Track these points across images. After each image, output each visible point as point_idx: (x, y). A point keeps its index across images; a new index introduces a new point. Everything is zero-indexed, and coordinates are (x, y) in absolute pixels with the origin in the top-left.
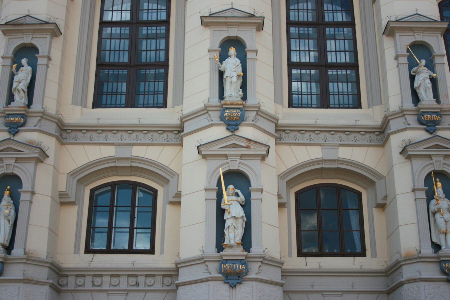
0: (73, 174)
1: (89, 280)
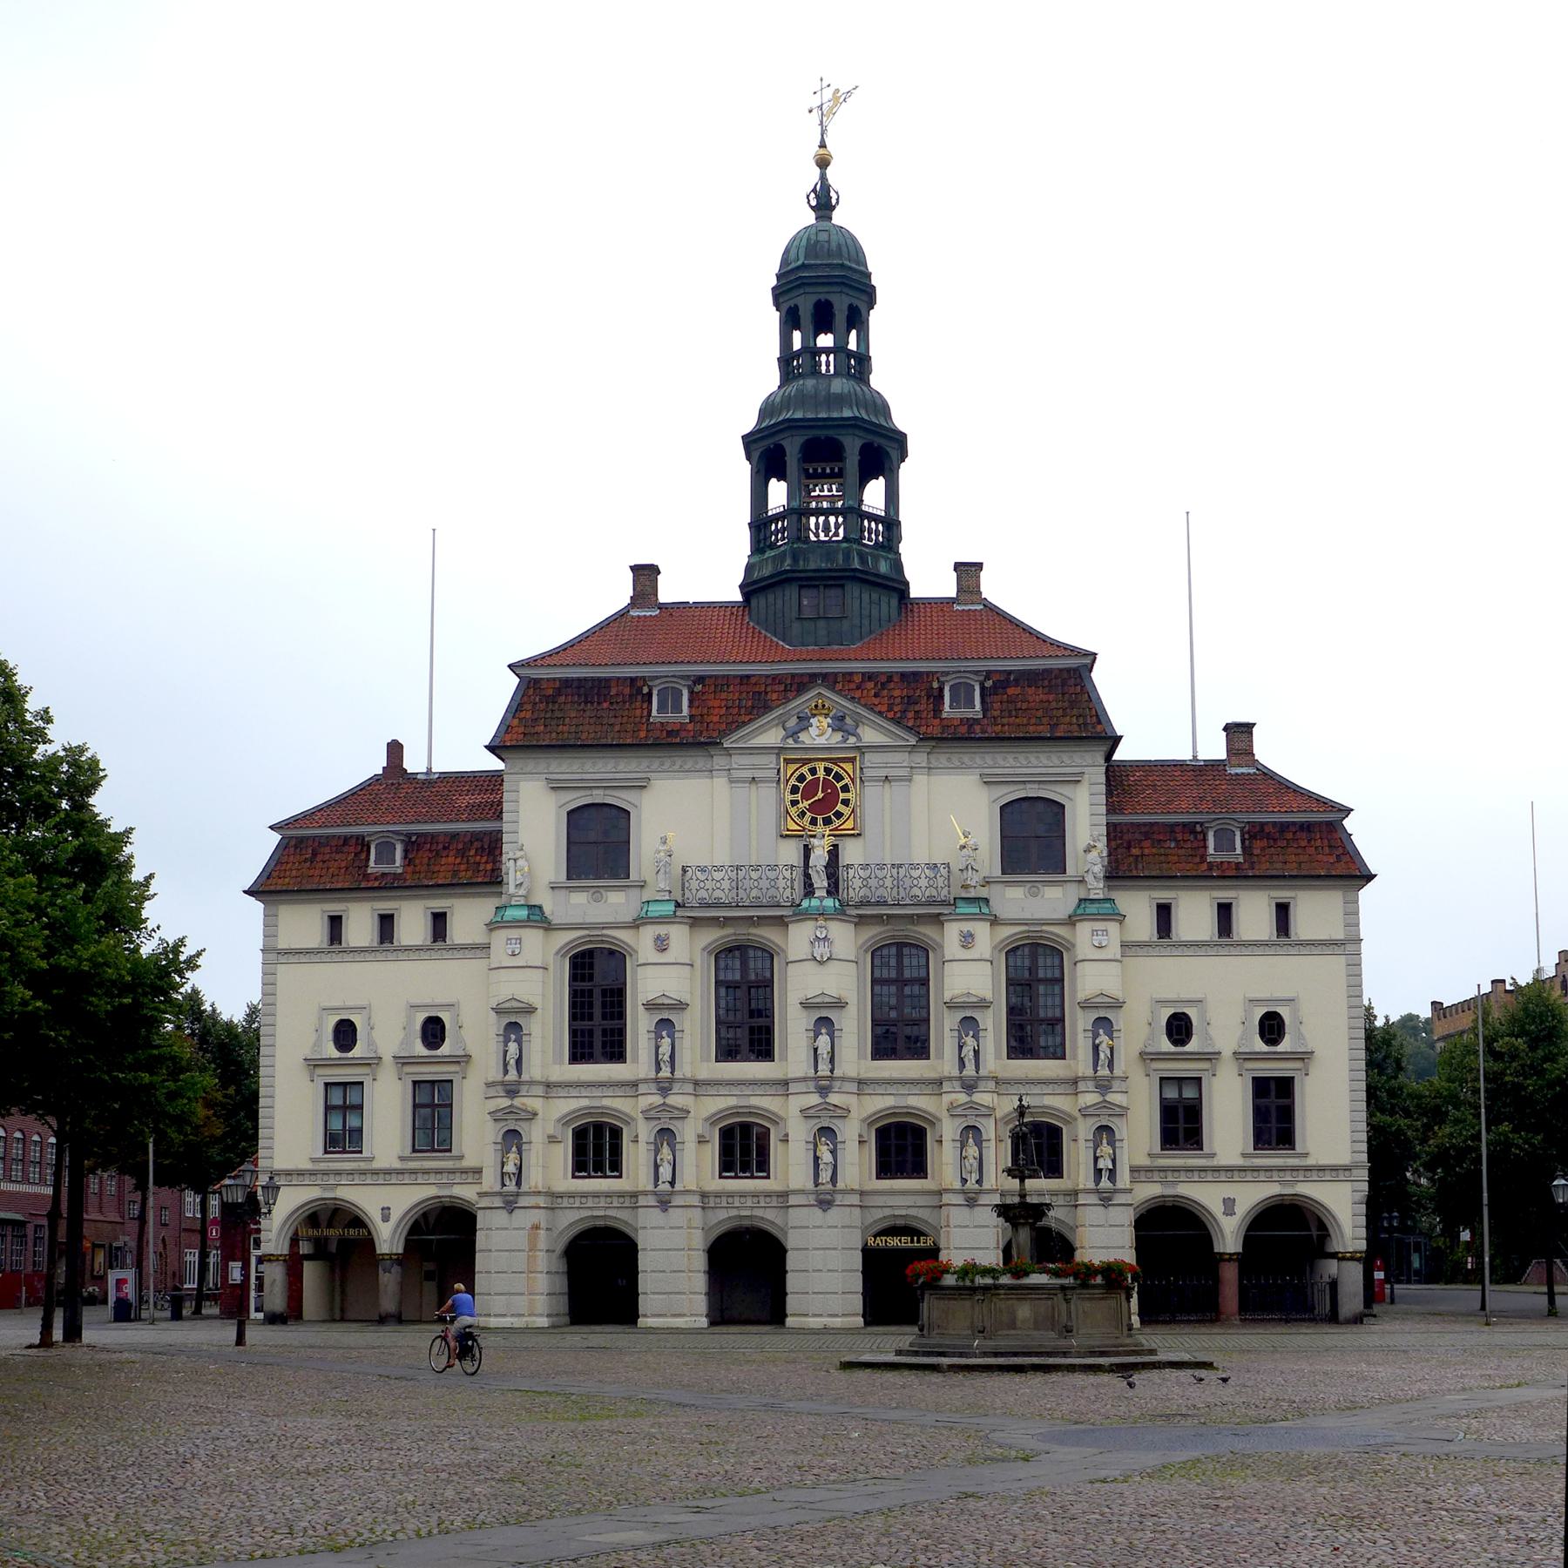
0: (706, 1120)
1: (724, 1199)
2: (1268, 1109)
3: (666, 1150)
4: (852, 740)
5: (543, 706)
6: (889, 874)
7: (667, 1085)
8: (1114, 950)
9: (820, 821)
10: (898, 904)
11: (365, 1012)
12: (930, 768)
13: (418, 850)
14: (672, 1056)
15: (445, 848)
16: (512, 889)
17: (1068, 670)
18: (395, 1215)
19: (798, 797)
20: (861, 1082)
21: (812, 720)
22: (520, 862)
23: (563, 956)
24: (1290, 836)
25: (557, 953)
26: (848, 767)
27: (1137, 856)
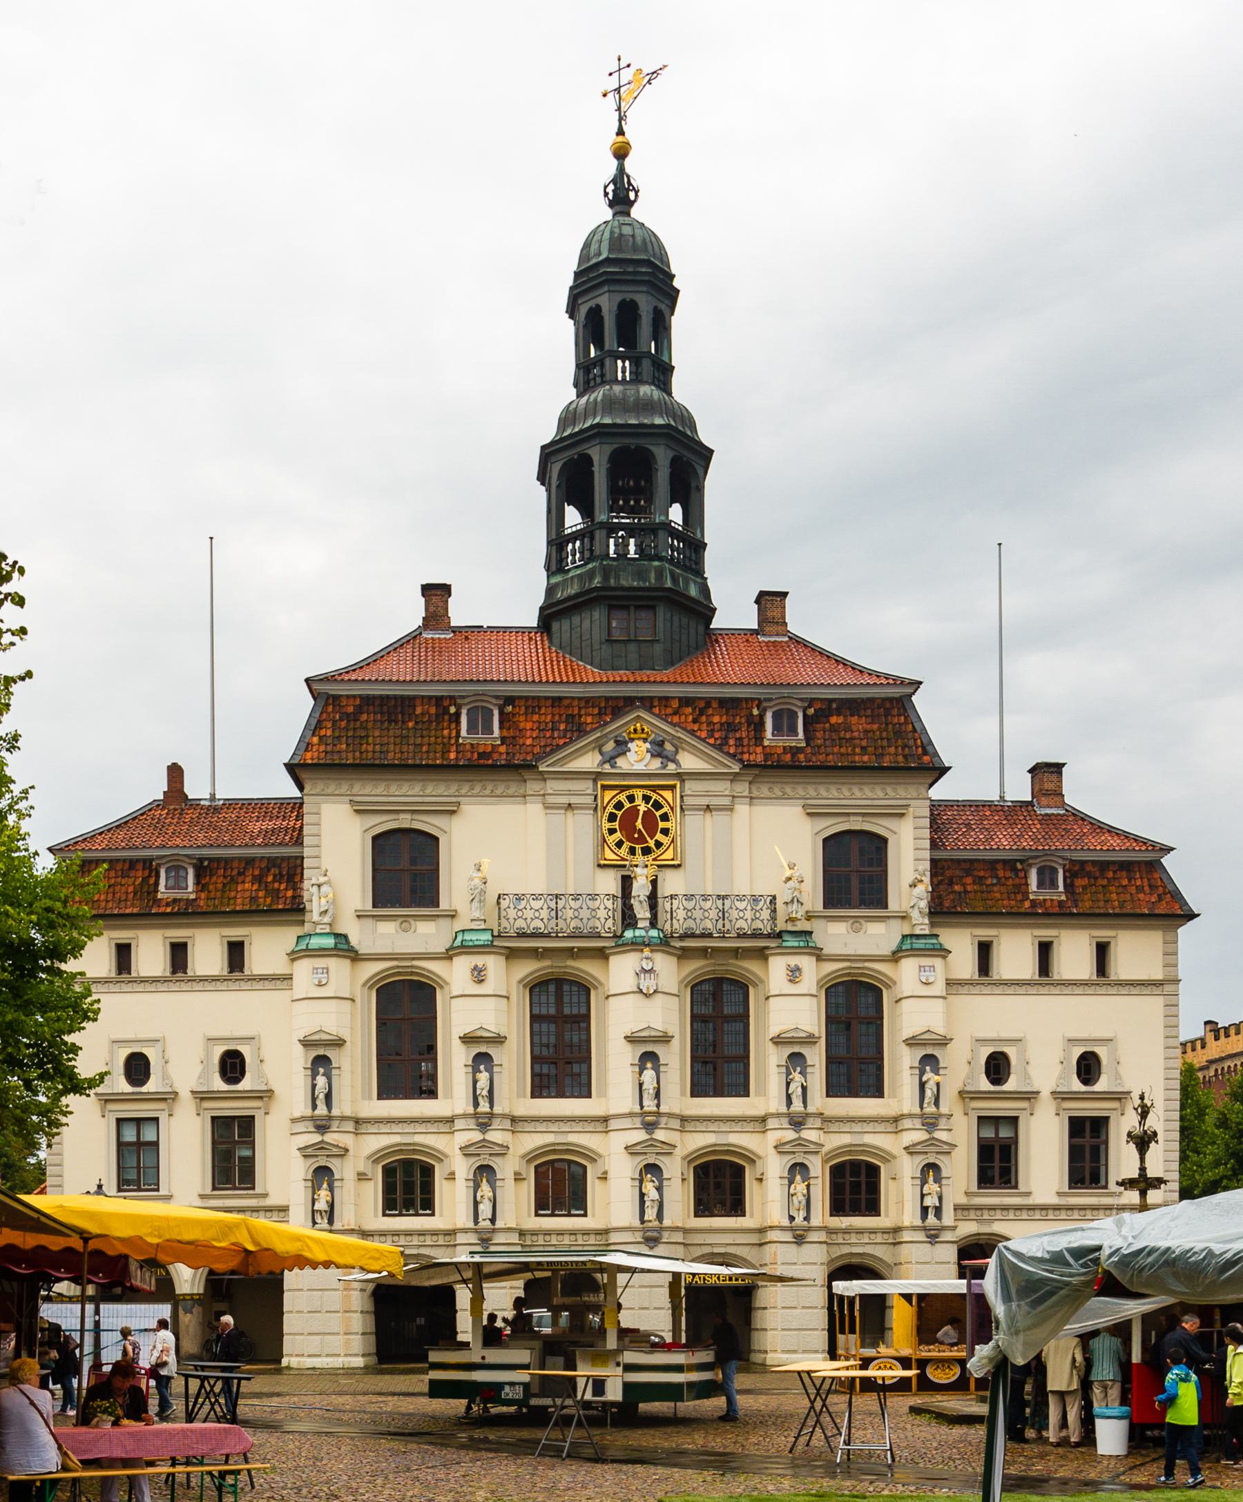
0: (523, 1157)
2: (1082, 1147)
3: (485, 1189)
4: (671, 767)
5: (343, 724)
6: (714, 906)
7: (486, 1120)
8: (939, 988)
9: (639, 851)
10: (724, 937)
11: (159, 1045)
12: (751, 798)
13: (211, 876)
14: (491, 1091)
15: (240, 874)
16: (316, 917)
17: (891, 700)
19: (616, 825)
20: (684, 1119)
21: (630, 745)
22: (324, 889)
23: (370, 988)
24: (1111, 875)
25: (364, 985)
26: (667, 794)
27: (960, 893)
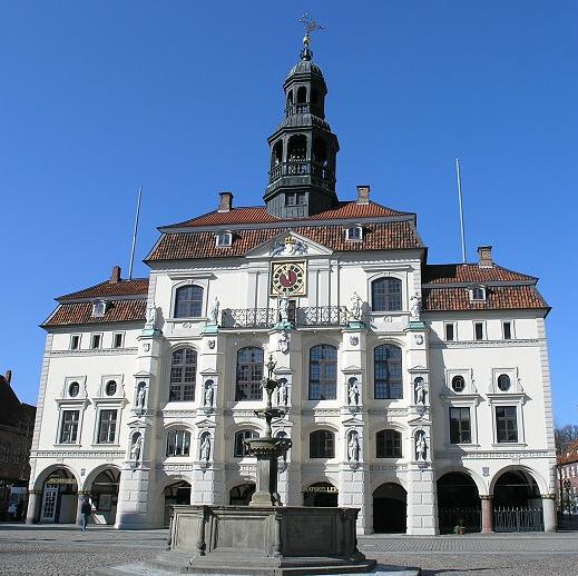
18: (87, 474)
26: (301, 265)
